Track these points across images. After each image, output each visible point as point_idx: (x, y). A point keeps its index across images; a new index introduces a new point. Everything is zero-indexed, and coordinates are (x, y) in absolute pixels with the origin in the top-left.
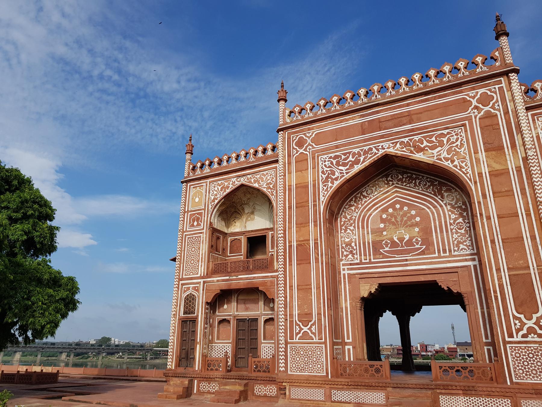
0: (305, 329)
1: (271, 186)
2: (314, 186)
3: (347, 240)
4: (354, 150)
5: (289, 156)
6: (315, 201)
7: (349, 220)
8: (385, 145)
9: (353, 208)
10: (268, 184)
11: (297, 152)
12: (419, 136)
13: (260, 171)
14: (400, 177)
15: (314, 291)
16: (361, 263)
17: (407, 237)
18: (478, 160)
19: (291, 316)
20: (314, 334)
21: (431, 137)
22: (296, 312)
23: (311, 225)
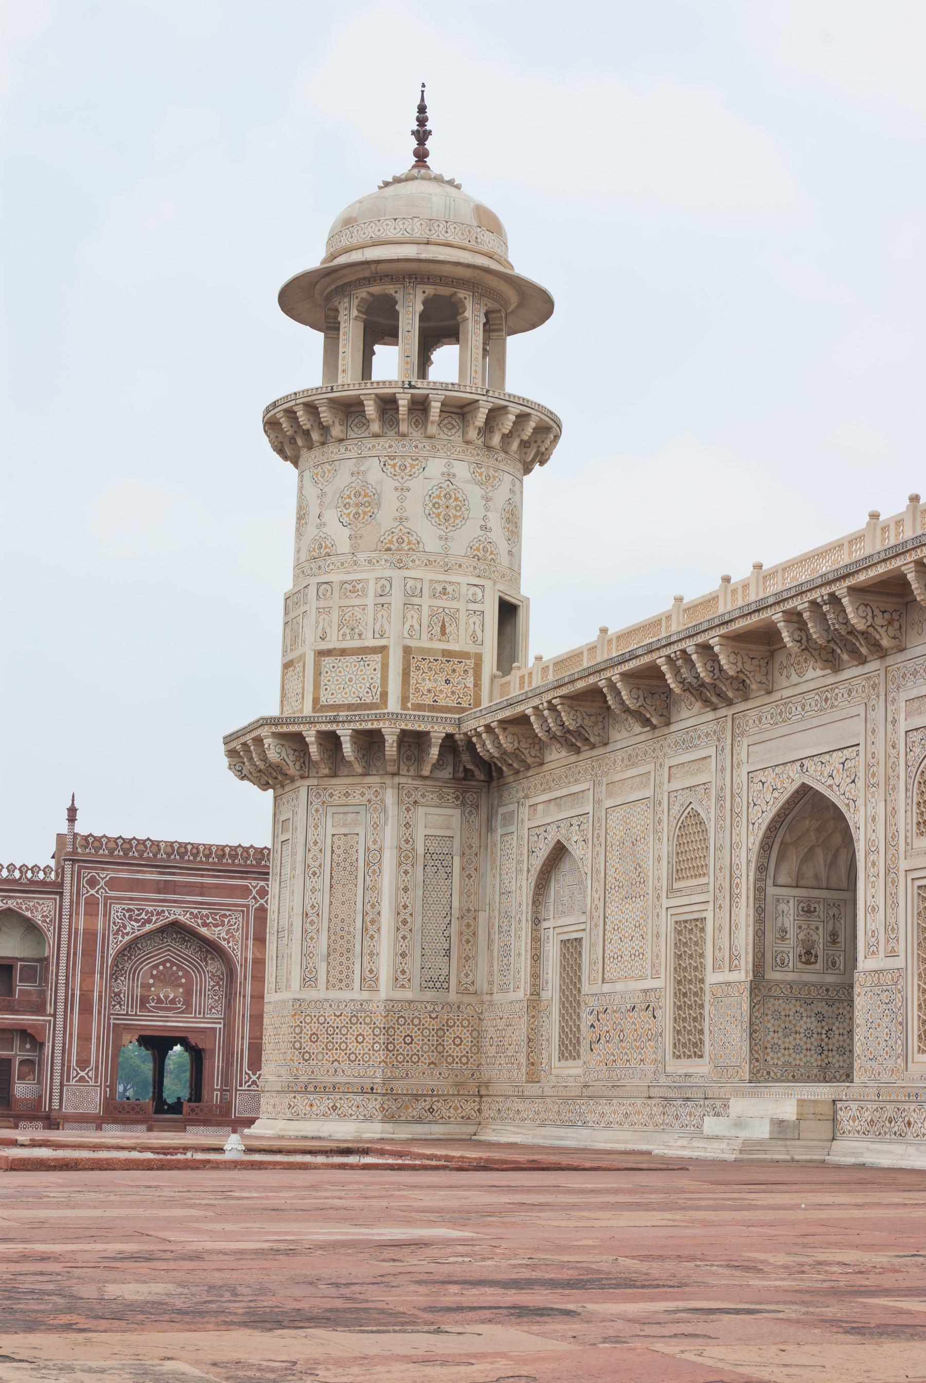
0: (82, 1074)
1: (48, 920)
2: (104, 935)
3: (116, 990)
4: (148, 908)
5: (78, 894)
6: (103, 952)
7: (121, 970)
8: (178, 911)
9: (126, 958)
10: (43, 916)
11: (88, 892)
12: (207, 911)
13: (34, 898)
14: (175, 936)
15: (94, 1040)
16: (127, 1014)
17: (172, 996)
18: (247, 946)
19: (69, 1061)
20: (91, 1078)
21: (216, 914)
22: (74, 1058)
23: (97, 976)
